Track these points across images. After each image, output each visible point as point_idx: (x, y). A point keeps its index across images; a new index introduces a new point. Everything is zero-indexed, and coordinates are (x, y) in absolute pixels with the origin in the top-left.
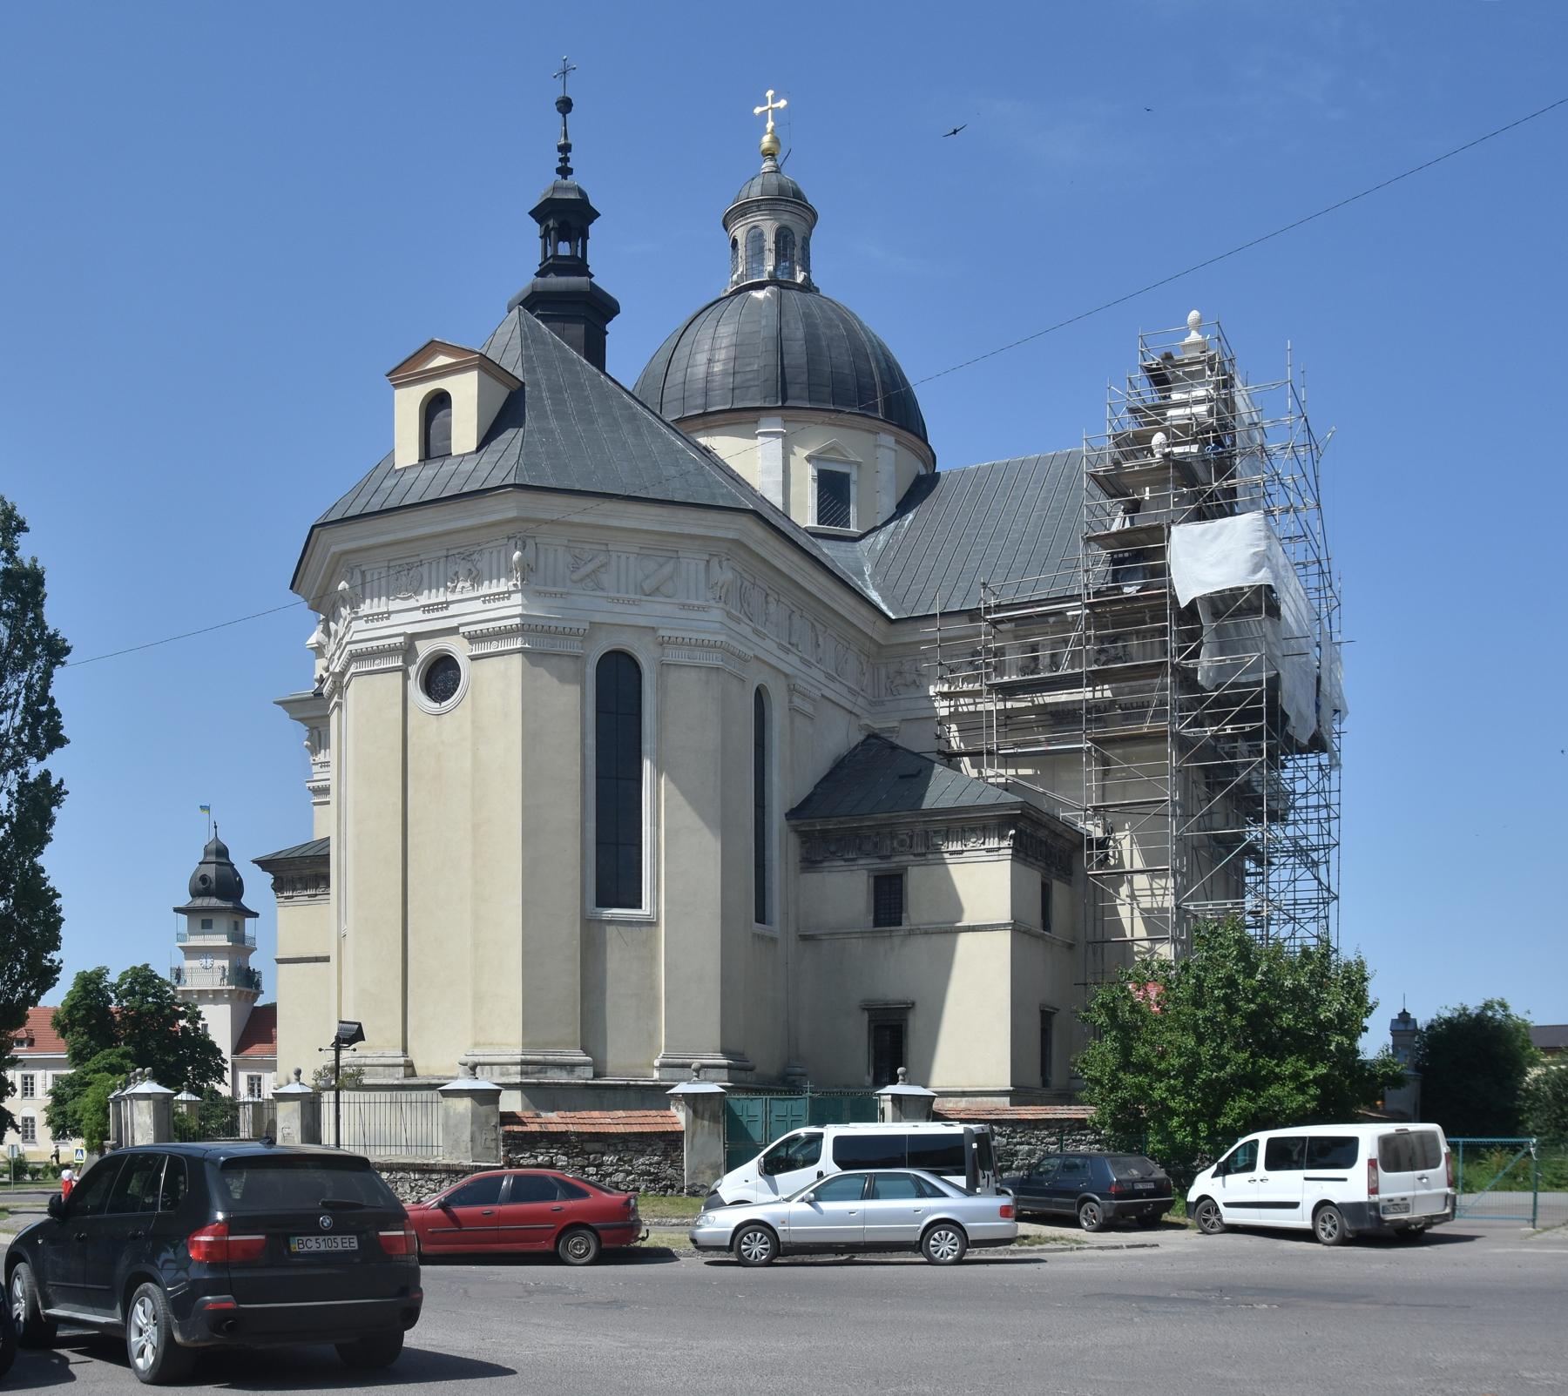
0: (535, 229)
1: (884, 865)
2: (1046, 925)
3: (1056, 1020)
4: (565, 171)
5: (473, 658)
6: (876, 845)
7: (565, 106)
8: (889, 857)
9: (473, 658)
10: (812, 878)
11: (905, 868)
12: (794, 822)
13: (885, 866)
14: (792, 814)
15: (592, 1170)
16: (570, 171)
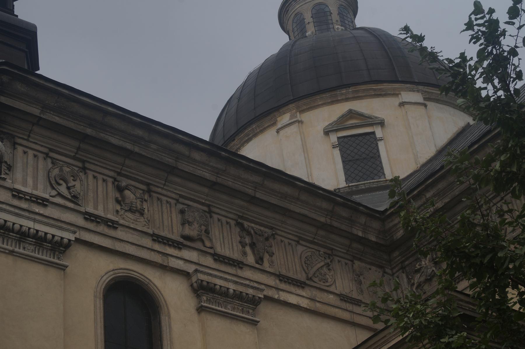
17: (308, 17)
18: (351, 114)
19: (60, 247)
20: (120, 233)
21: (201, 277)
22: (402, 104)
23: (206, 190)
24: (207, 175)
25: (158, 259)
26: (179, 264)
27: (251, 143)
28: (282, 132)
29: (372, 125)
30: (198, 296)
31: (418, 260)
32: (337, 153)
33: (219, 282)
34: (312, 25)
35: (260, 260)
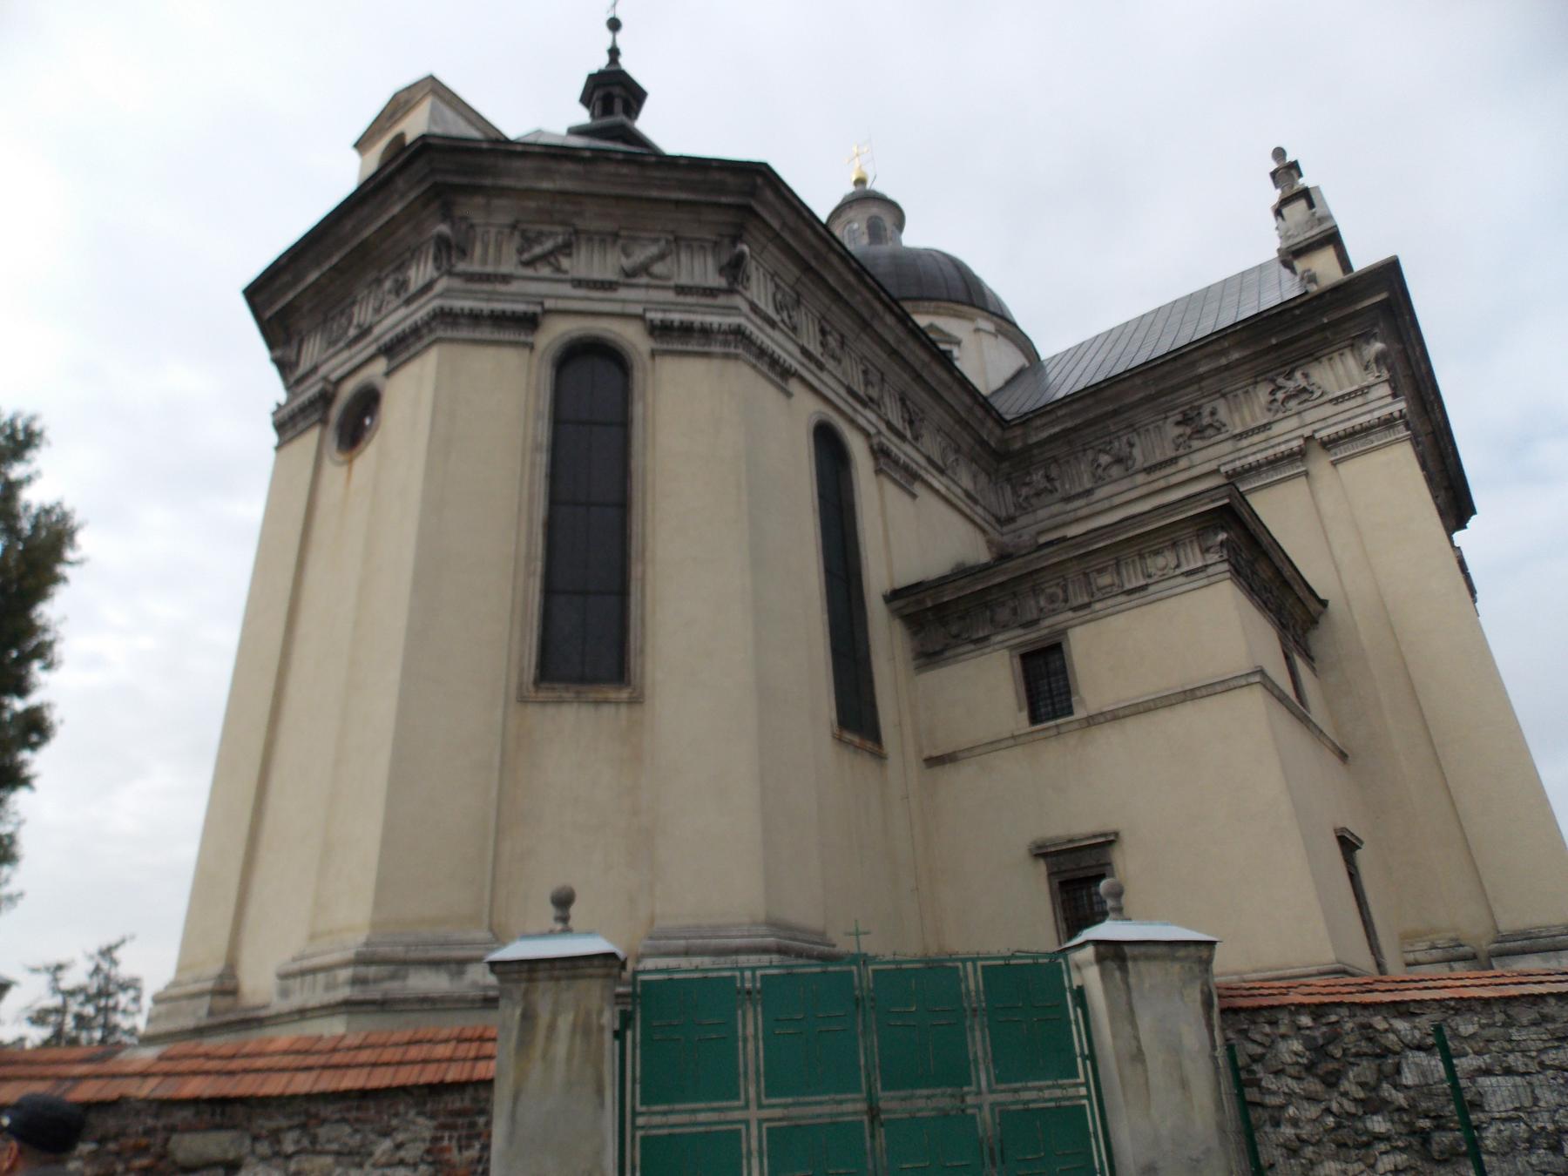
1: (1032, 635)
6: (1014, 611)
8: (1033, 623)
11: (1064, 632)
12: (898, 603)
13: (1033, 636)
14: (893, 596)
19: (786, 373)
20: (825, 376)
22: (977, 330)
23: (884, 356)
24: (892, 341)
25: (849, 410)
30: (876, 459)
31: (1029, 474)
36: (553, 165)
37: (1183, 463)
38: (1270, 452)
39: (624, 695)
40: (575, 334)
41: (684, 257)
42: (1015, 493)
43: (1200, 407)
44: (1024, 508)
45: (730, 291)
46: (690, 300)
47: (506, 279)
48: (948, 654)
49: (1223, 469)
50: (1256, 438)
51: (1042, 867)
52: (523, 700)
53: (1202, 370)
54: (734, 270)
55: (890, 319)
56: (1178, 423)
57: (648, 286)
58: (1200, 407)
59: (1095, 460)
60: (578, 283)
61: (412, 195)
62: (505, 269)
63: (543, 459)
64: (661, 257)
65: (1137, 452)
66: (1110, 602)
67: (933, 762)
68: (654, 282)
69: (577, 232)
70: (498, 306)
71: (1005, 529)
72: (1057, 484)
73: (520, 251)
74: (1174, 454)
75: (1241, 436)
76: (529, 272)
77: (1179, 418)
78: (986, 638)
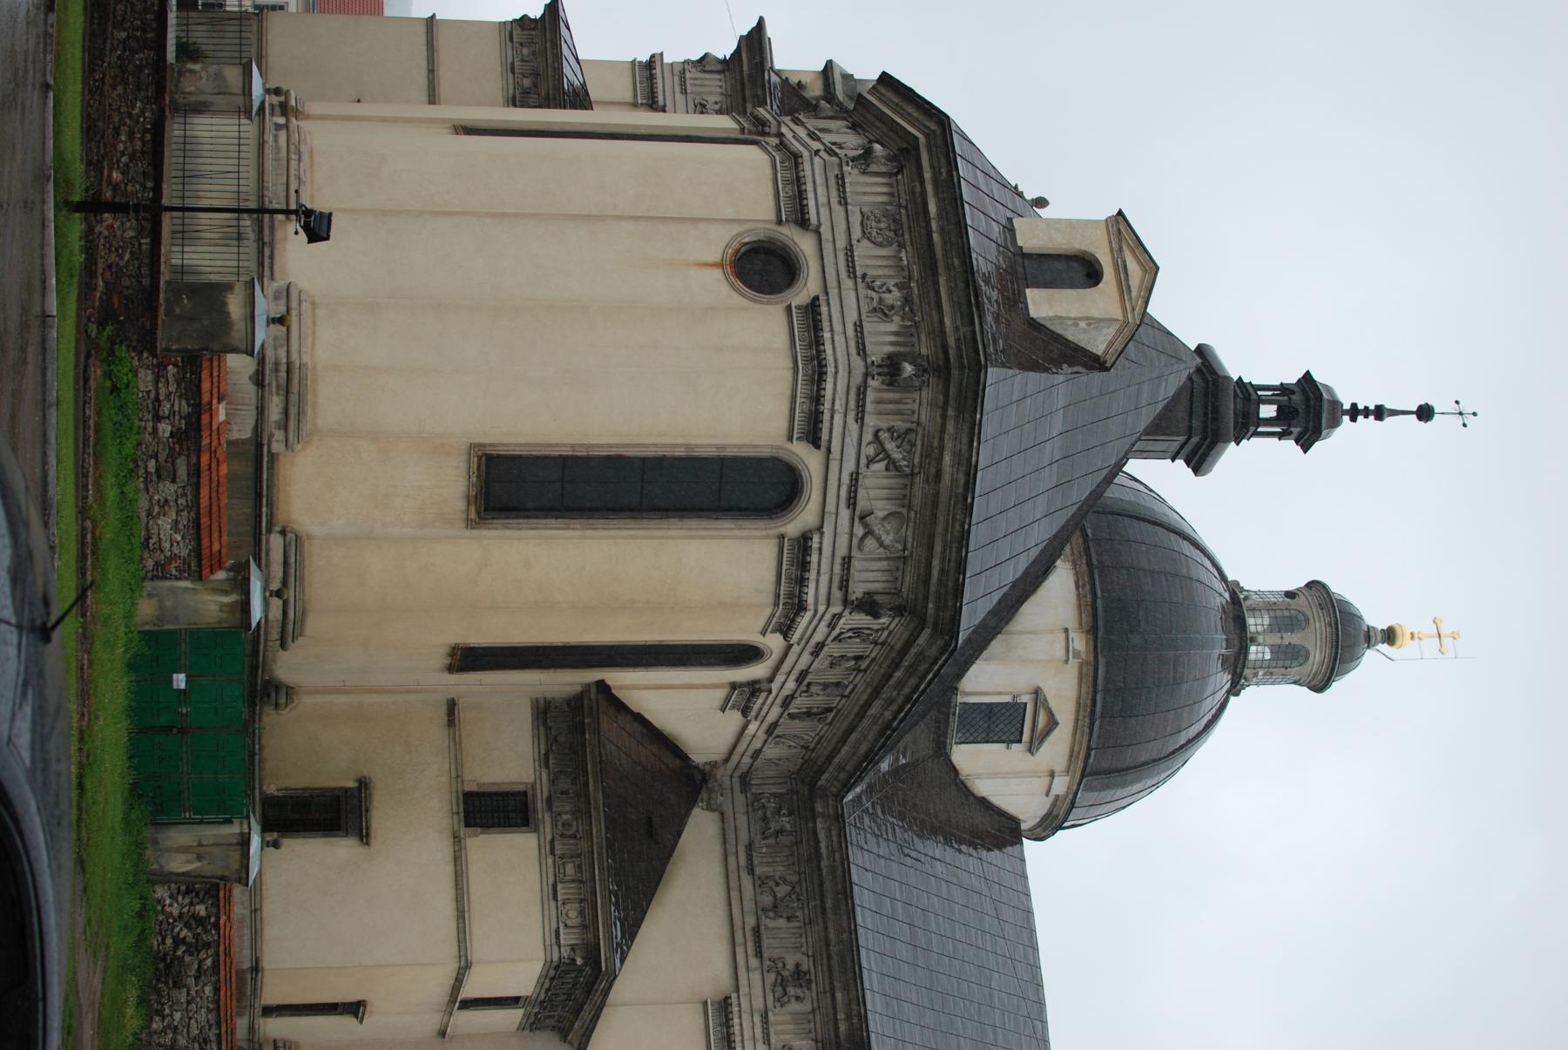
0: (1292, 378)
1: (540, 805)
2: (468, 1004)
3: (348, 1022)
4: (1354, 413)
5: (789, 308)
7: (1425, 413)
8: (550, 809)
9: (789, 308)
10: (525, 715)
11: (536, 830)
12: (593, 690)
14: (602, 686)
15: (152, 465)
16: (1353, 419)
17: (1290, 638)
18: (1052, 723)
20: (806, 658)
21: (764, 695)
22: (1052, 775)
26: (780, 678)
27: (1073, 585)
28: (1062, 636)
29: (1031, 742)
32: (1007, 699)
33: (760, 701)
34: (1278, 641)
35: (792, 716)
36: (963, 468)
37: (754, 962)
38: (738, 1039)
39: (473, 515)
40: (805, 474)
41: (885, 563)
42: (774, 795)
43: (810, 989)
44: (755, 803)
45: (846, 602)
46: (837, 568)
47: (860, 419)
48: (542, 730)
49: (734, 995)
50: (758, 1031)
51: (352, 784)
52: (473, 446)
53: (839, 996)
54: (868, 605)
55: (888, 714)
56: (798, 965)
57: (851, 534)
58: (810, 989)
59: (785, 881)
60: (855, 478)
61: (951, 341)
62: (871, 421)
63: (680, 452)
64: (881, 545)
65: (782, 922)
66: (551, 871)
67: (452, 706)
68: (855, 542)
69: (912, 474)
70: (826, 417)
71: (736, 780)
72: (771, 841)
73: (890, 430)
74: (766, 955)
75: (765, 1016)
76: (868, 437)
77: (804, 968)
78: (547, 767)
